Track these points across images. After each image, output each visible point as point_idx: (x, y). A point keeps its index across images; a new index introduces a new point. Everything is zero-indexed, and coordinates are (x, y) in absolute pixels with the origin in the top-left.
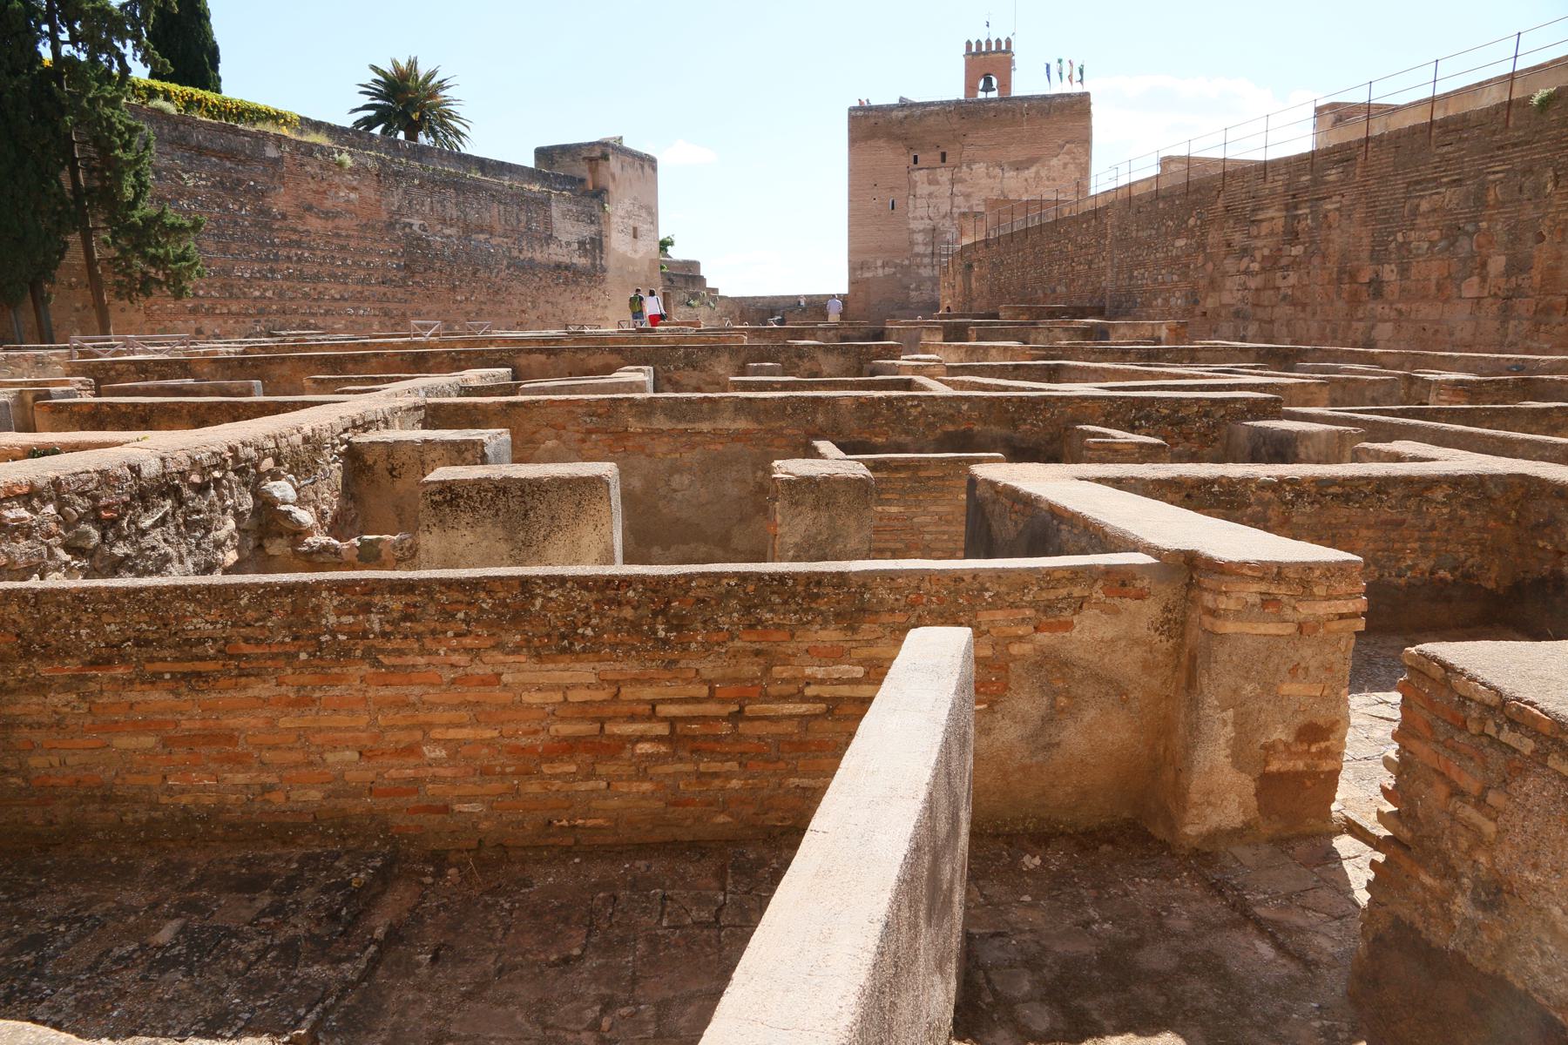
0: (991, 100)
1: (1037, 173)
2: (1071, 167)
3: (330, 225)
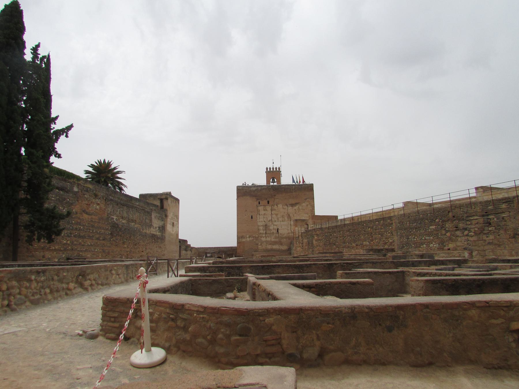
0: (275, 185)
1: (299, 207)
2: (309, 206)
3: (90, 217)
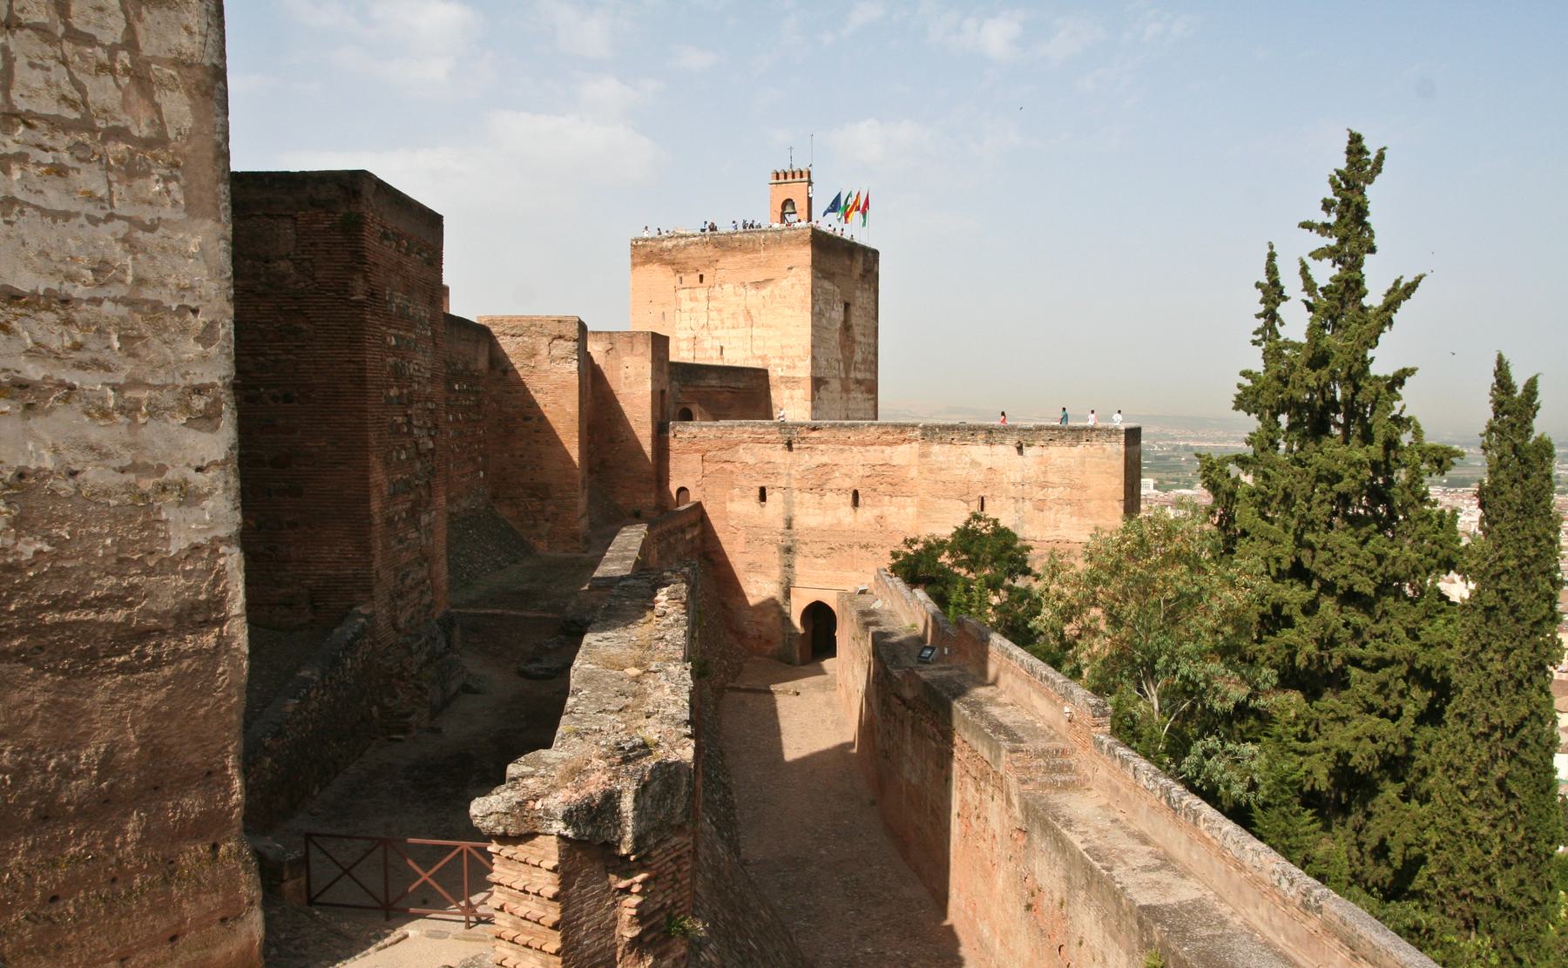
2: (797, 287)
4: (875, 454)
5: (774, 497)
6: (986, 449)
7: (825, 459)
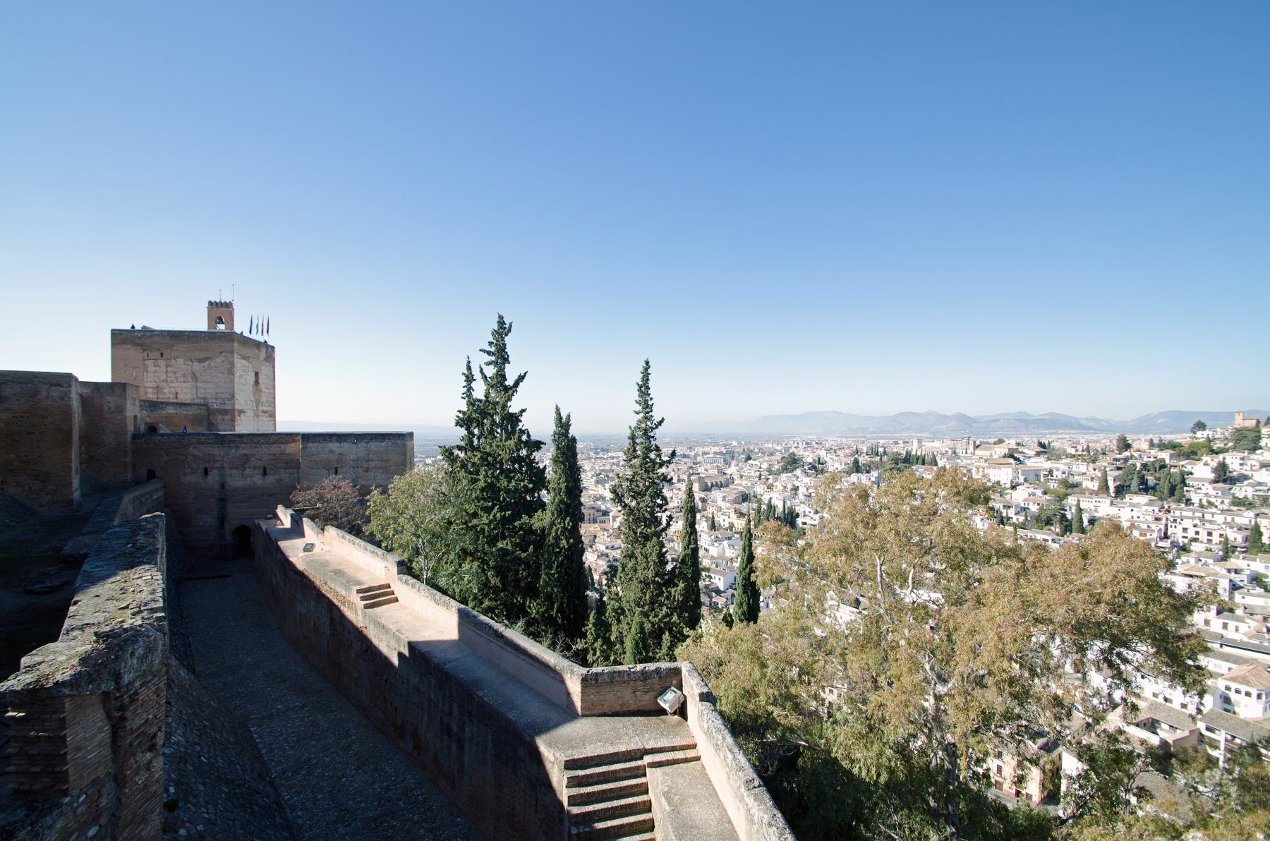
4: (275, 449)
5: (214, 474)
6: (337, 444)
7: (245, 452)
